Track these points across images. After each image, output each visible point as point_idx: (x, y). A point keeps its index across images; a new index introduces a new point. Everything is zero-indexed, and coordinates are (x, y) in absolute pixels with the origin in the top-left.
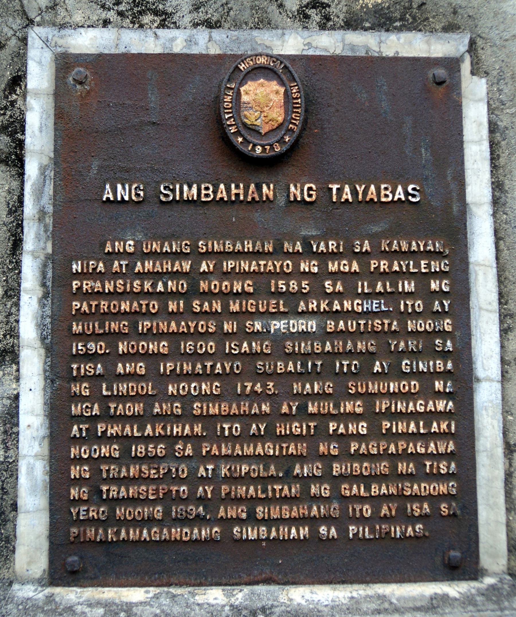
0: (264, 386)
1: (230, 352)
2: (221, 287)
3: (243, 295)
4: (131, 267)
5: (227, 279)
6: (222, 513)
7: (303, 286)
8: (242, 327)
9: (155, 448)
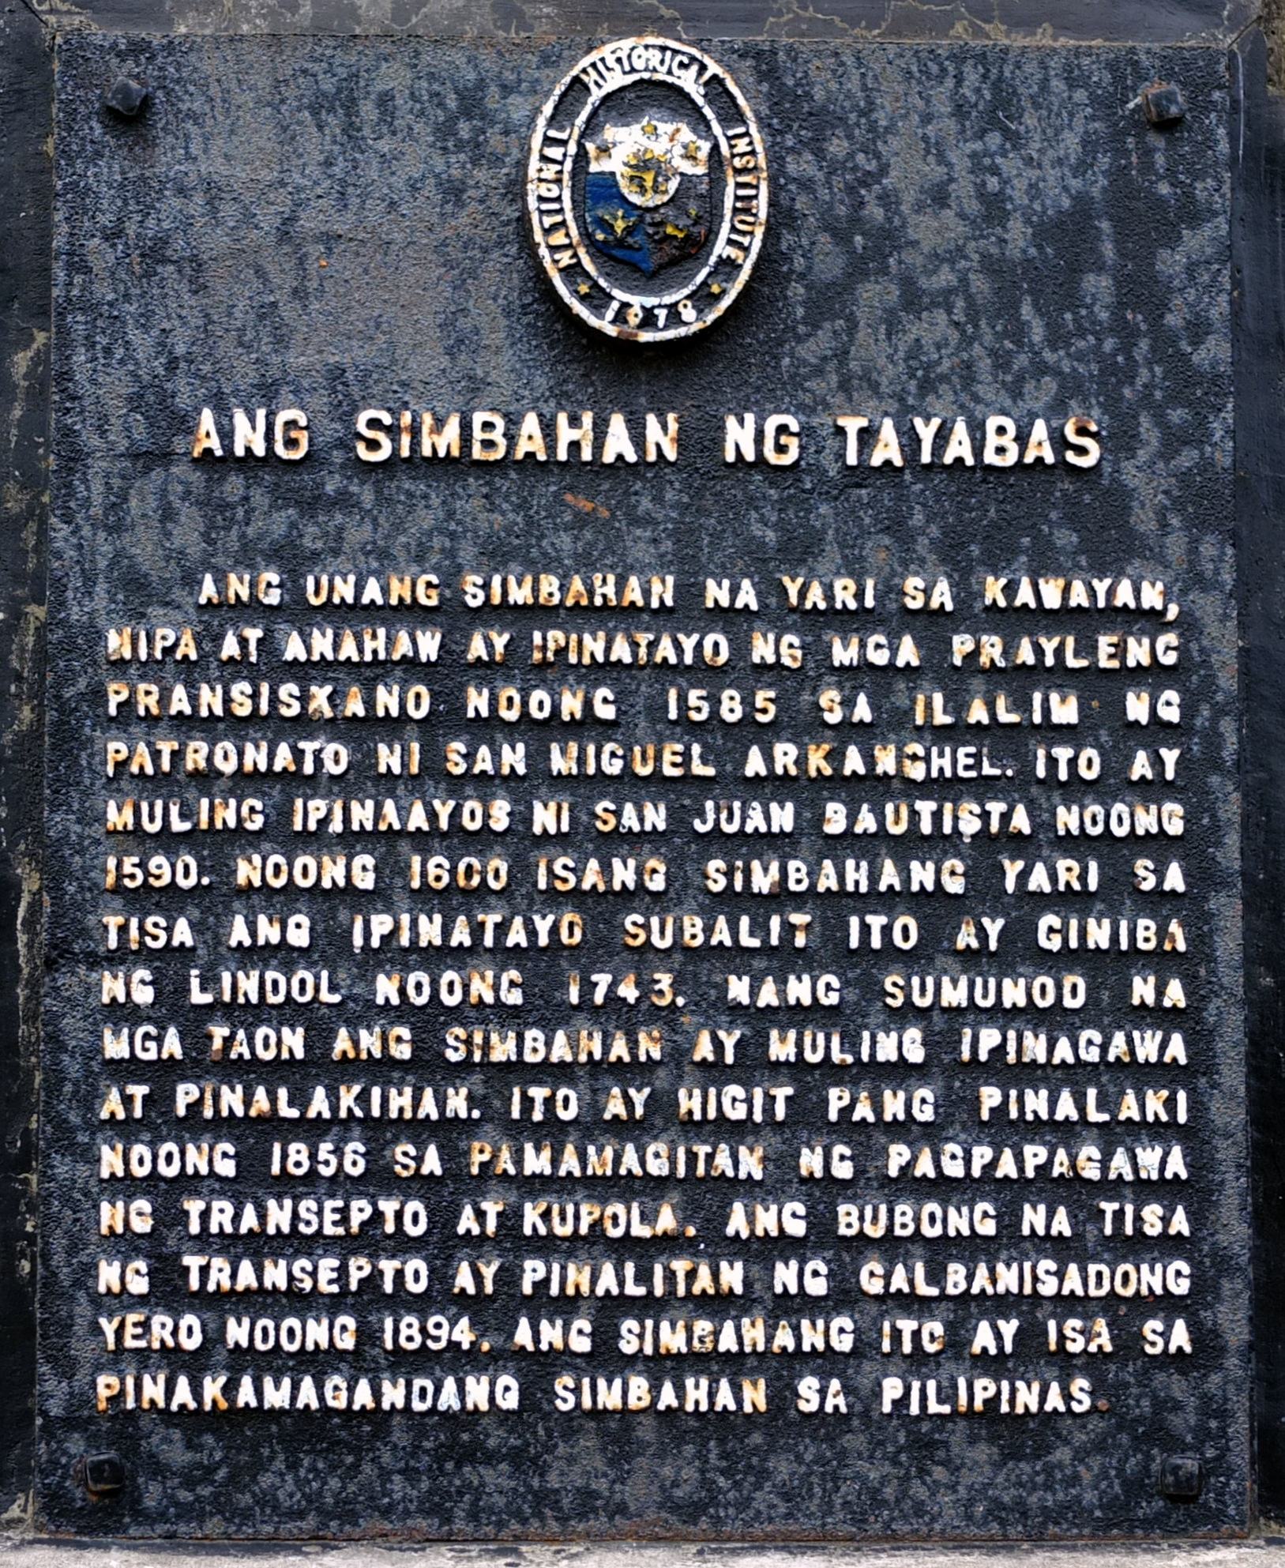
0: (645, 986)
2: (525, 704)
3: (587, 726)
5: (543, 683)
6: (523, 1336)
7: (759, 704)
9: (338, 1152)
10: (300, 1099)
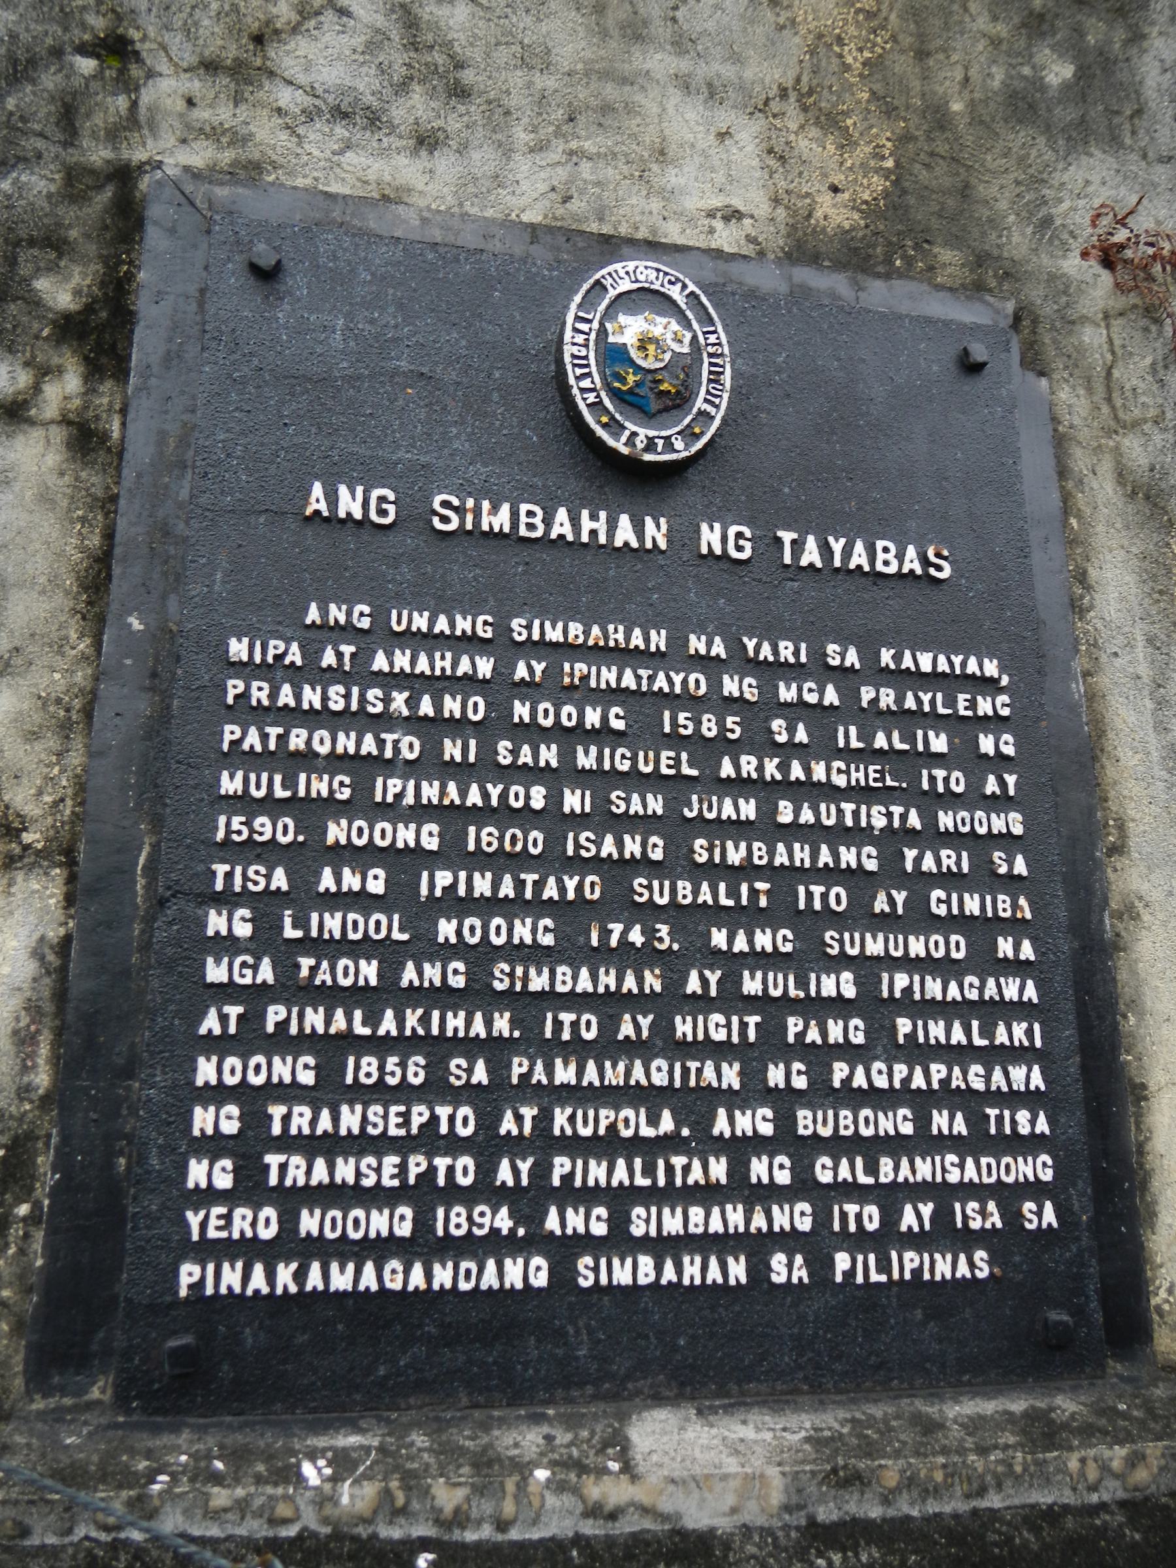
0: (650, 933)
1: (577, 854)
2: (557, 715)
3: (603, 735)
4: (362, 658)
6: (552, 1223)
7: (729, 725)
8: (602, 803)
9: (403, 1065)
10: (373, 1019)
